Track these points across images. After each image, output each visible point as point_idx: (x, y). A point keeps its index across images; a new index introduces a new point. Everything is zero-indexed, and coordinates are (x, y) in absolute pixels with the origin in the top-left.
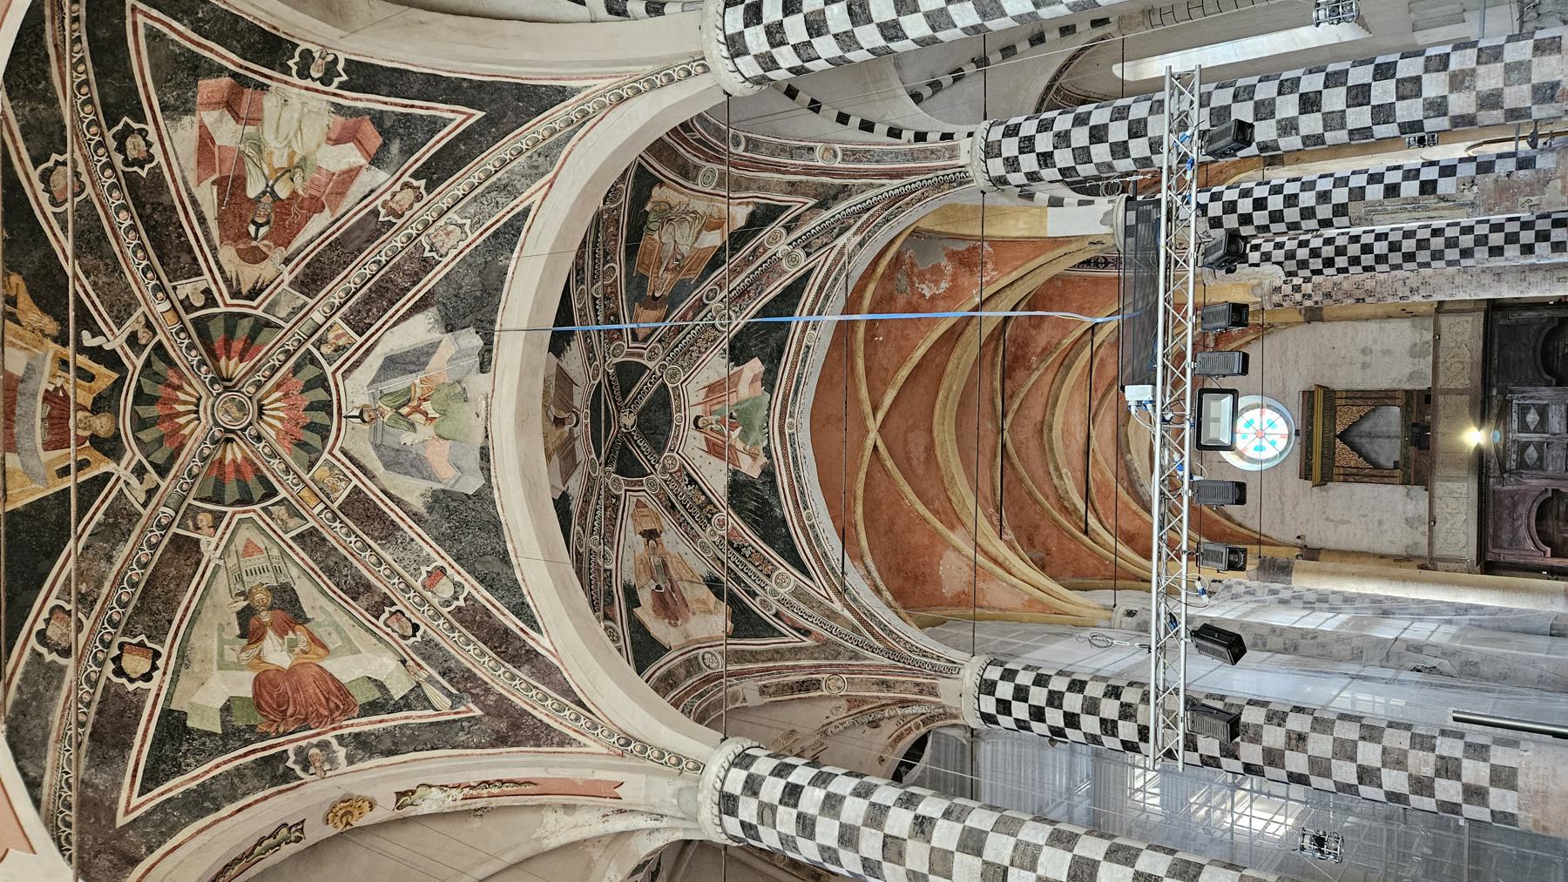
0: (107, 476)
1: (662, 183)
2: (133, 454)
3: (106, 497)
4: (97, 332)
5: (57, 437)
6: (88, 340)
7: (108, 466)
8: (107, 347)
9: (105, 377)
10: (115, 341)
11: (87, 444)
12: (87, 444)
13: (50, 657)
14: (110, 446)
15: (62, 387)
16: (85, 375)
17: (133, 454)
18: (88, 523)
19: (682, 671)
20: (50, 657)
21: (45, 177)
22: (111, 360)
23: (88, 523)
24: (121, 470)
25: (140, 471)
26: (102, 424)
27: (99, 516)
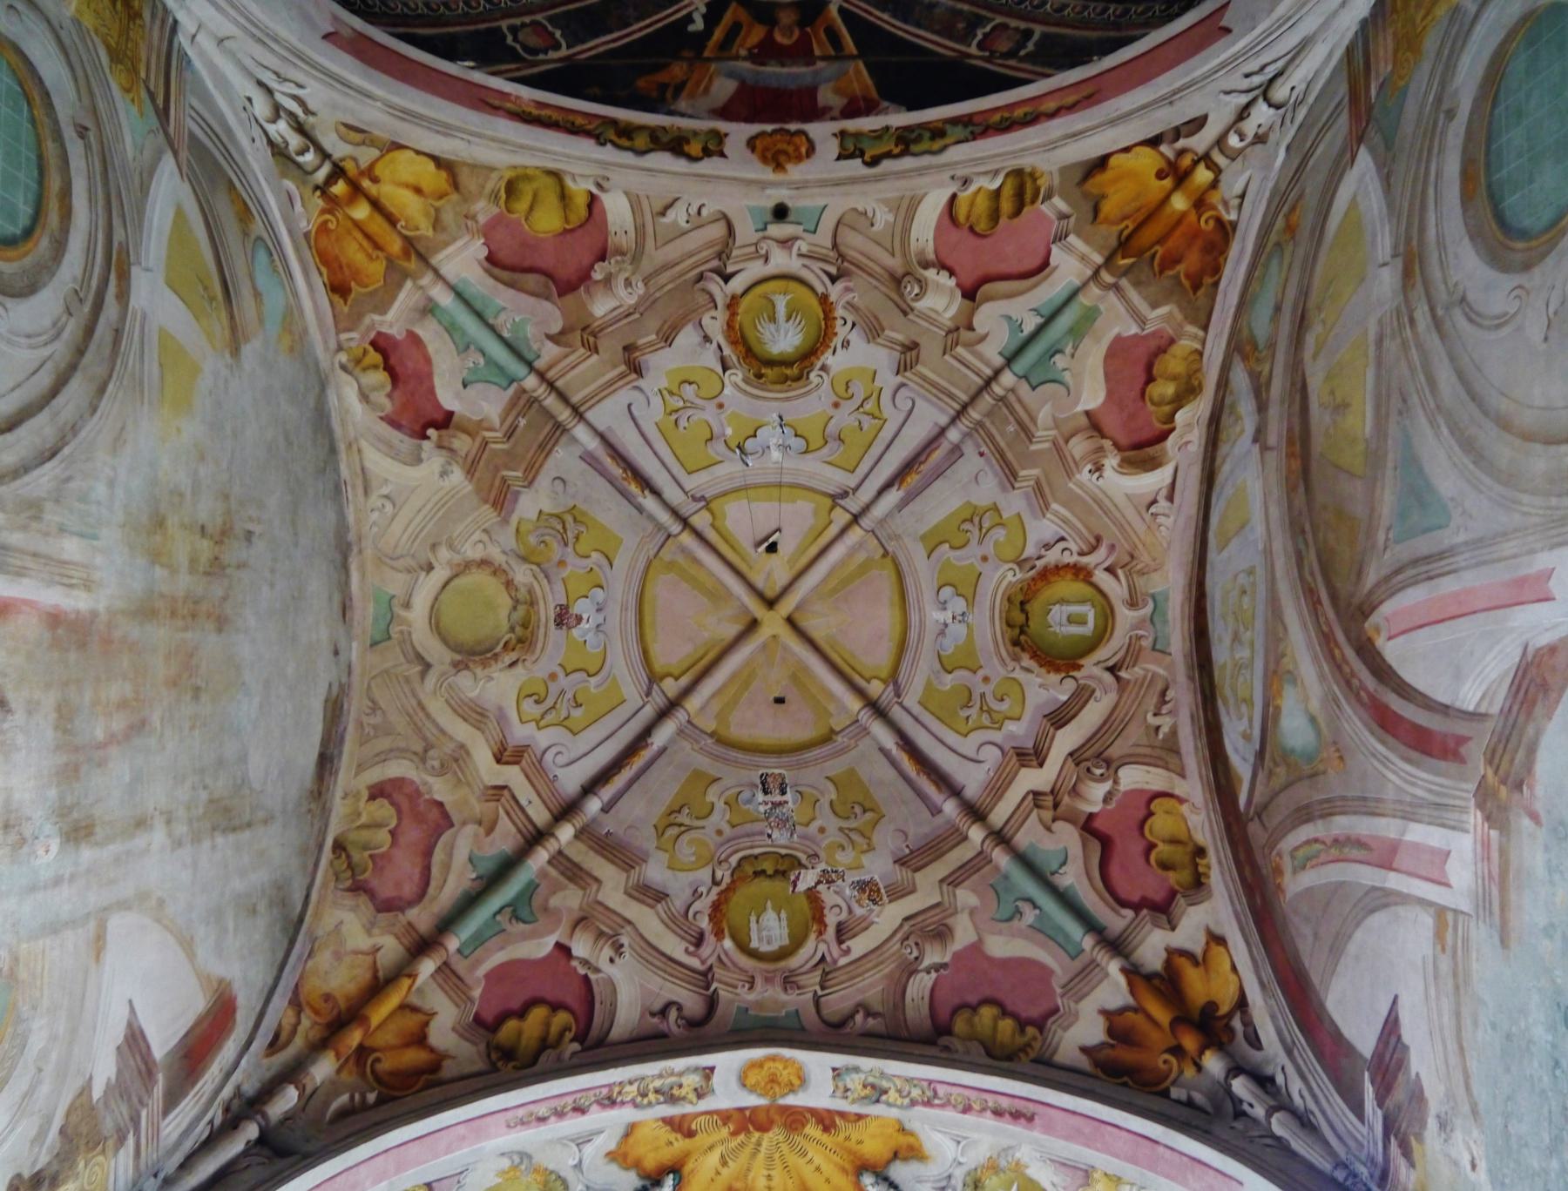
0: (841, 10)
3: (866, 11)
4: (689, 19)
5: (801, 52)
6: (698, 25)
8: (703, 10)
11: (809, 29)
12: (809, 29)
15: (749, 50)
18: (893, 26)
23: (893, 26)
27: (885, 16)
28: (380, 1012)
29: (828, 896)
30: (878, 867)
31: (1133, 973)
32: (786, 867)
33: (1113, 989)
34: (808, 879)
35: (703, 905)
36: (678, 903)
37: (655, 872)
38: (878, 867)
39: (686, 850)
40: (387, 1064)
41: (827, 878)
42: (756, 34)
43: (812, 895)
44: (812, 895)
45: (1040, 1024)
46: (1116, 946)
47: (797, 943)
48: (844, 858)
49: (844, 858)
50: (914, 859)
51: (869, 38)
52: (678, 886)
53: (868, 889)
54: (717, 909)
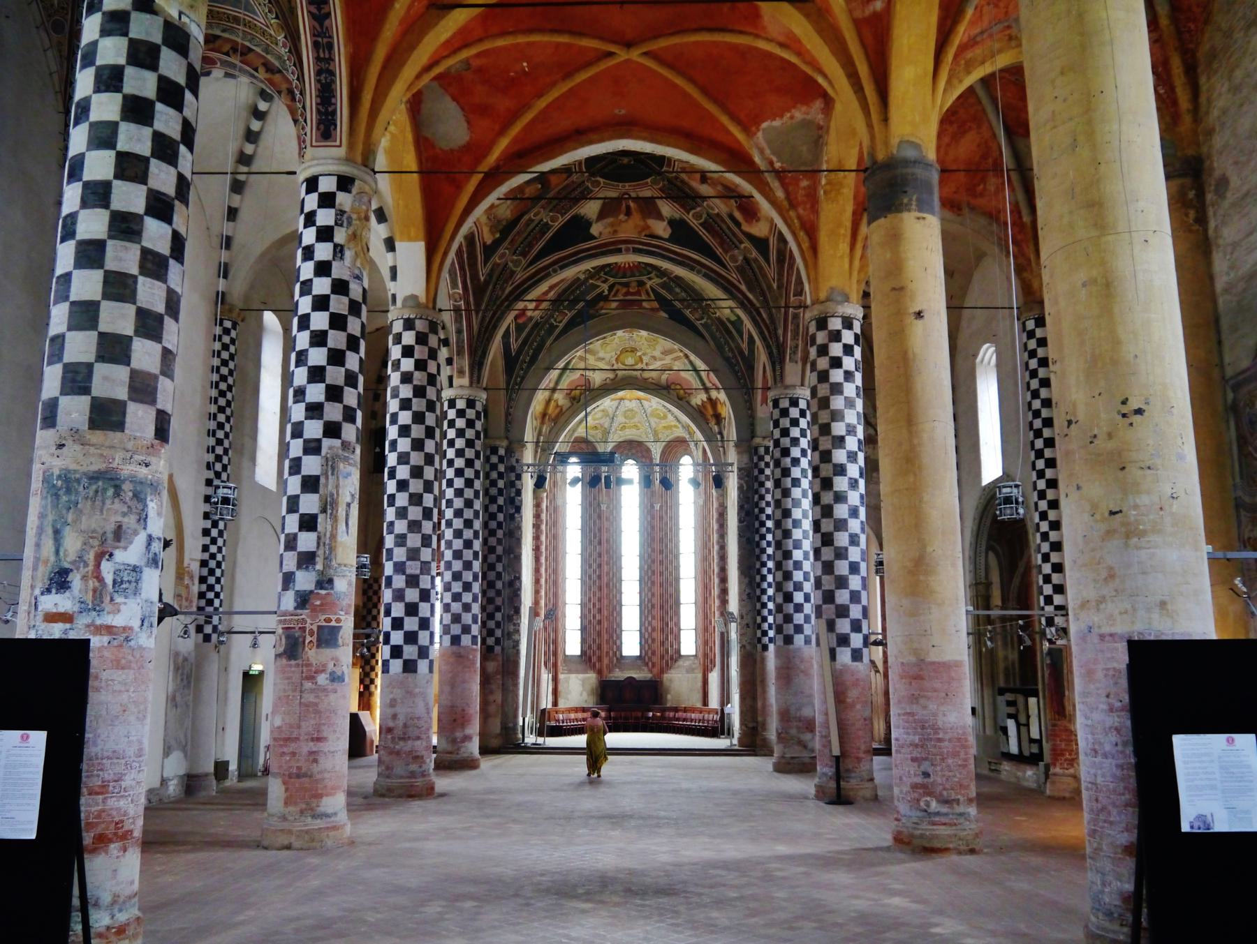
1: (484, 244)
2: (644, 278)
5: (638, 293)
6: (606, 293)
7: (648, 286)
9: (617, 287)
10: (605, 287)
13: (703, 322)
14: (641, 284)
16: (618, 291)
17: (644, 278)
19: (782, 245)
20: (703, 322)
21: (560, 322)
22: (611, 287)
24: (649, 284)
25: (650, 279)
26: (634, 284)
28: (550, 410)
29: (644, 358)
30: (657, 353)
31: (710, 399)
32: (633, 350)
33: (703, 396)
34: (639, 354)
35: (614, 359)
36: (607, 359)
37: (601, 355)
38: (657, 353)
39: (608, 348)
40: (553, 416)
41: (644, 354)
42: (624, 290)
43: (640, 357)
44: (640, 357)
45: (689, 394)
46: (707, 390)
47: (636, 364)
48: (648, 351)
49: (648, 351)
50: (666, 353)
51: (659, 298)
52: (607, 356)
53: (654, 358)
54: (617, 359)
